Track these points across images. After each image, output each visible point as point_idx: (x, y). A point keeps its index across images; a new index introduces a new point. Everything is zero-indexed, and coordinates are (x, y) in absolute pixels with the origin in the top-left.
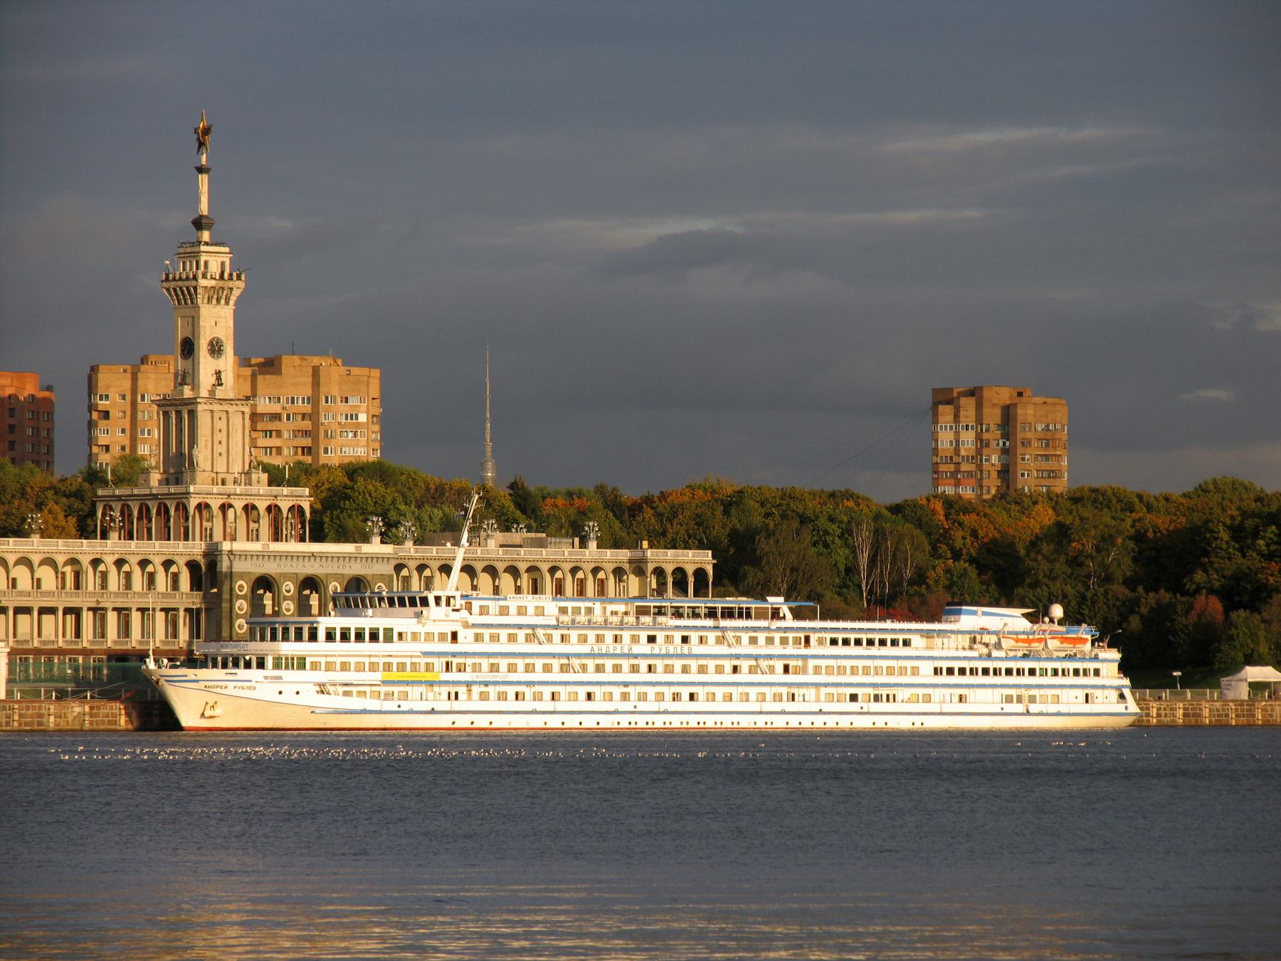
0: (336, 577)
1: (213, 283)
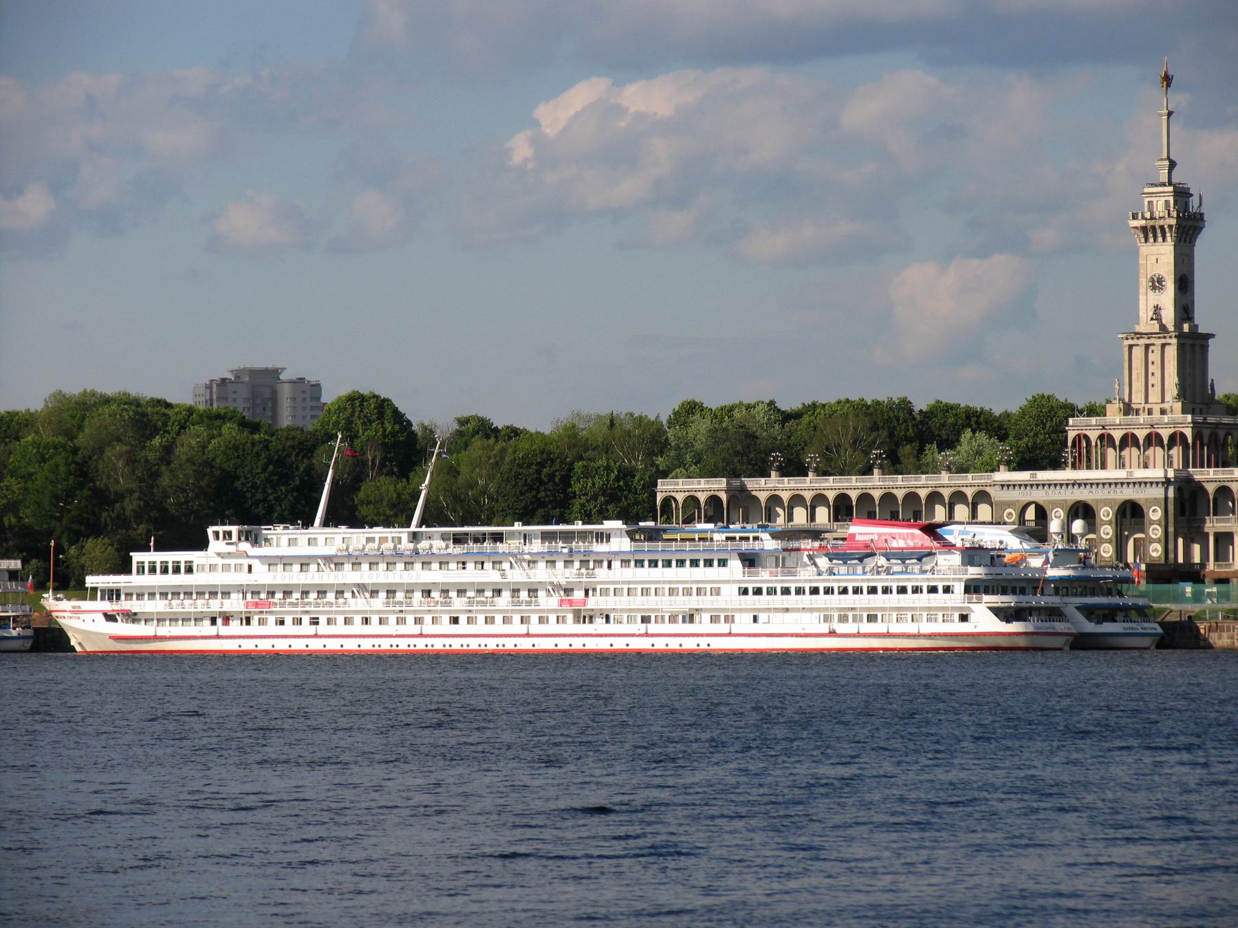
0: (1107, 502)
1: (1143, 223)
